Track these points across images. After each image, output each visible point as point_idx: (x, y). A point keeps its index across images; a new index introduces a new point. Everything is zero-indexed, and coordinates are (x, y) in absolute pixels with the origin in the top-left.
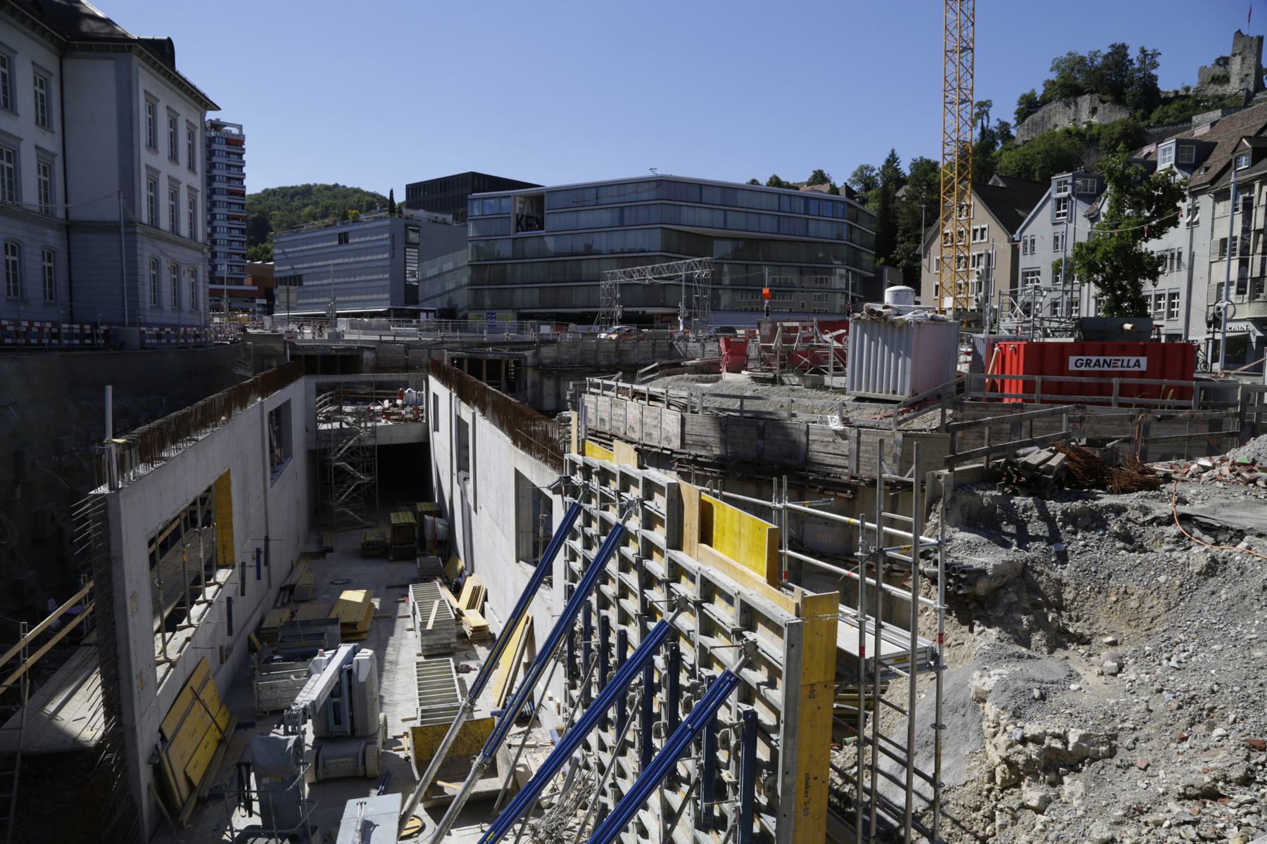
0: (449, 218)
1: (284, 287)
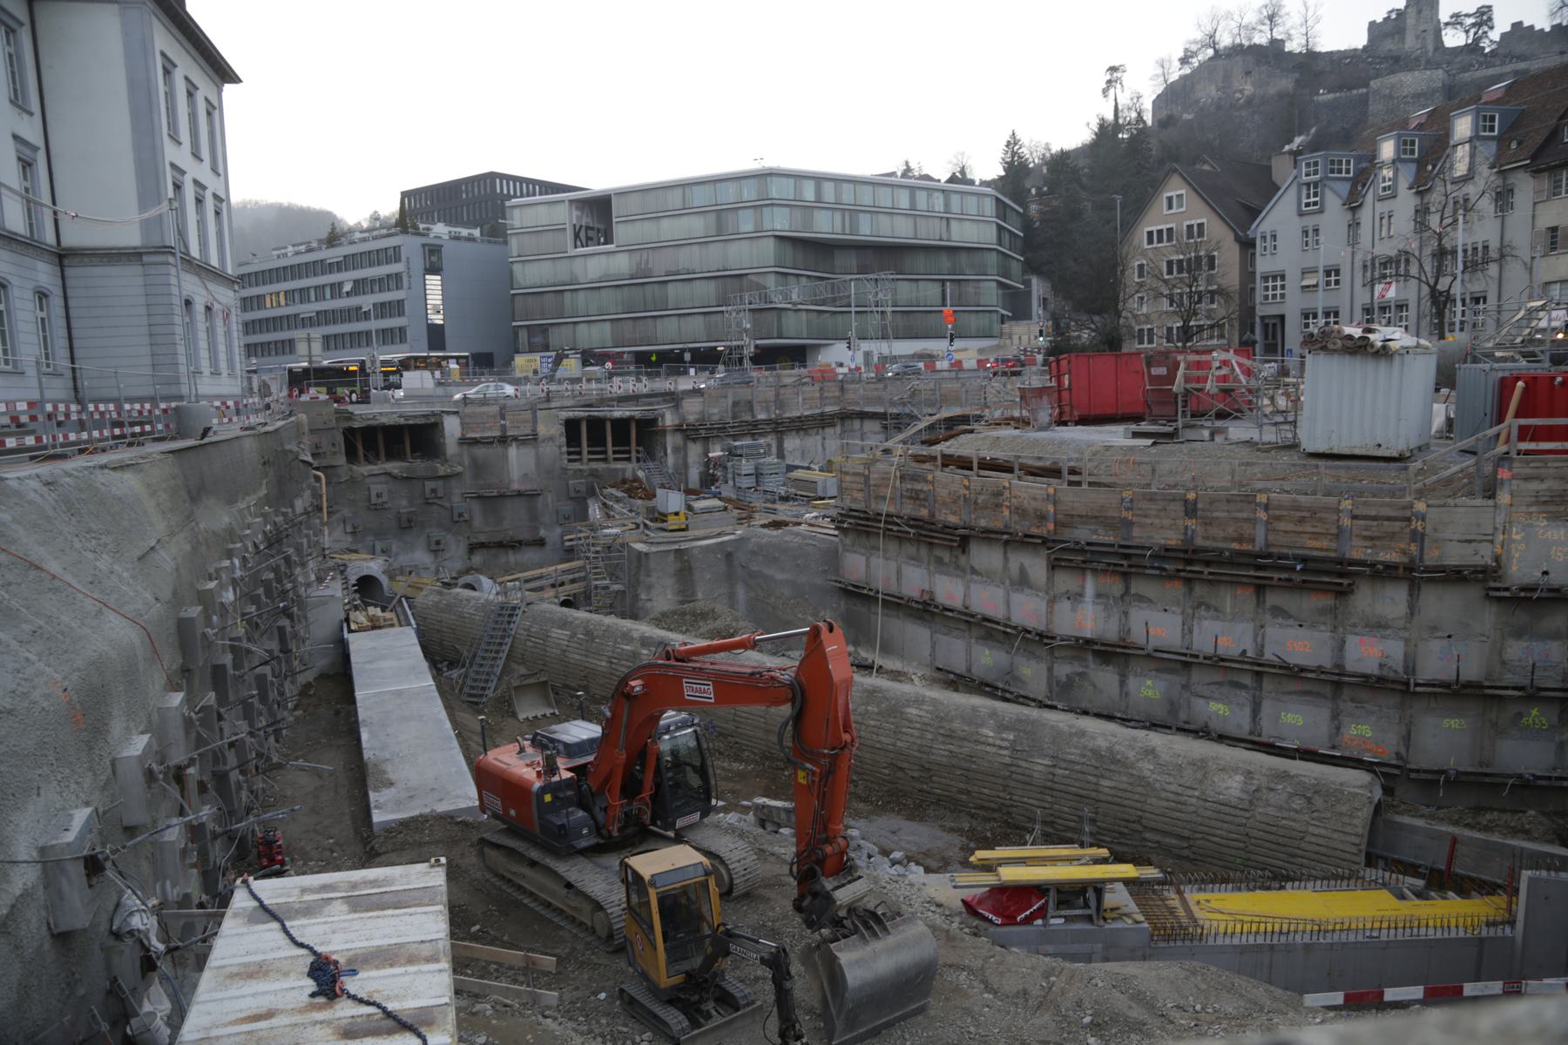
0: (477, 233)
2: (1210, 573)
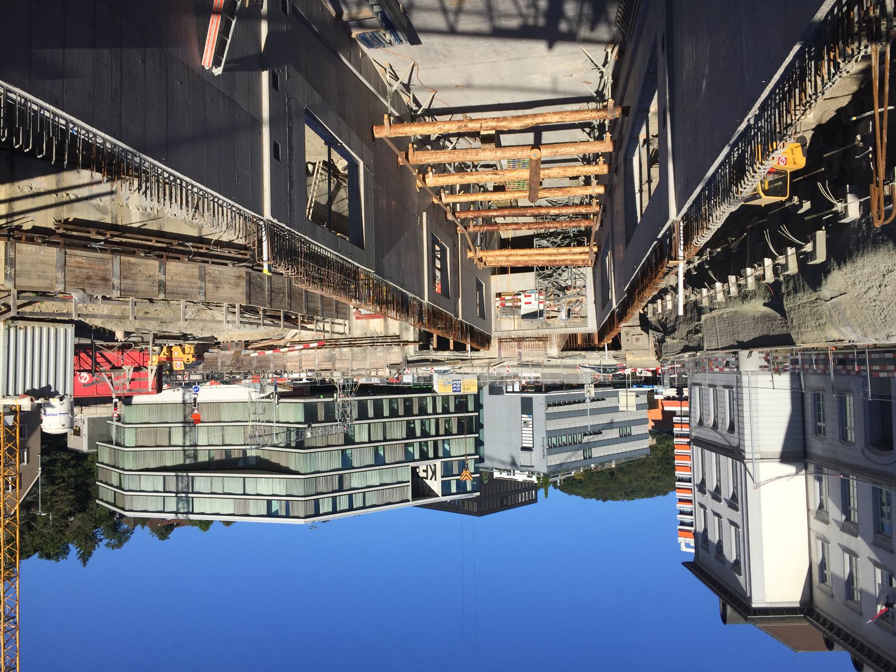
1: (629, 409)
2: (151, 241)
